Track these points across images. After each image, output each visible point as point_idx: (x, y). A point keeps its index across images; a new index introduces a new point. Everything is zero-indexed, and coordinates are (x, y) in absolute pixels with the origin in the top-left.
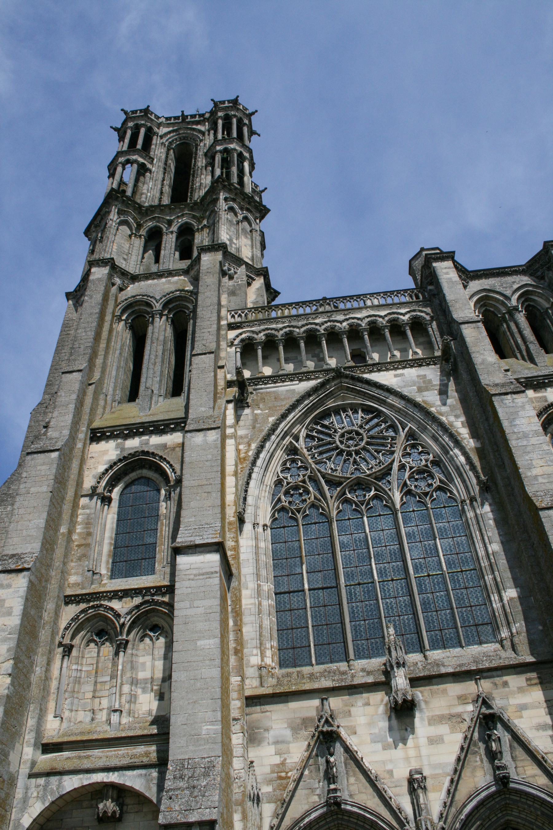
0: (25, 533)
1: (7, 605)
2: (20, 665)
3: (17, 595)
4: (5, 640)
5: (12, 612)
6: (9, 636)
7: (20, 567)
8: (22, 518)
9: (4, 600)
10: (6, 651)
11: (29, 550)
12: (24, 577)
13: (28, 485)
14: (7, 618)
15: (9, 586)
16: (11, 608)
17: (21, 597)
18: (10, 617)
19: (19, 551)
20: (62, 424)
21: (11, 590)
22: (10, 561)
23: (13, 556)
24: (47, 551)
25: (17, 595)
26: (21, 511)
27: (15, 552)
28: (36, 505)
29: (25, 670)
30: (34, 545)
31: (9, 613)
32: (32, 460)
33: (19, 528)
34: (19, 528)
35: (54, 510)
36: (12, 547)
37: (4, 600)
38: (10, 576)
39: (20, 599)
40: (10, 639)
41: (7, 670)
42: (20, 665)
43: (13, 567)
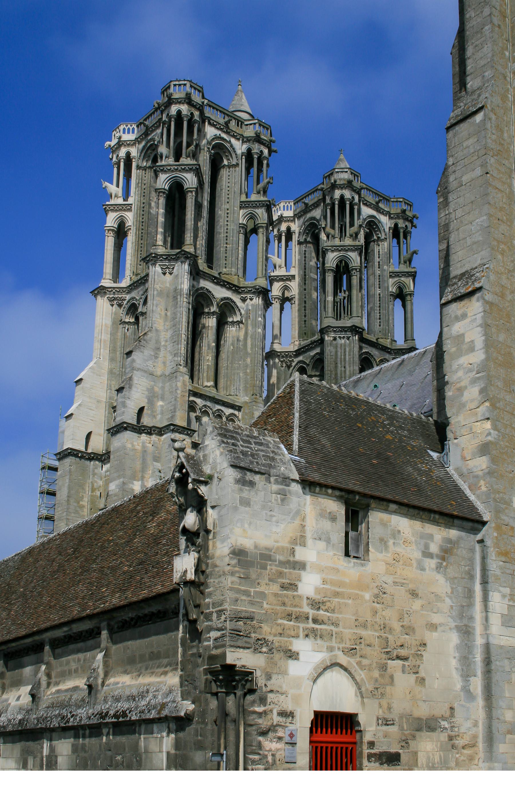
0: (469, 241)
1: (467, 339)
2: (500, 405)
3: (475, 324)
4: (474, 381)
5: (474, 347)
6: (477, 375)
7: (470, 289)
8: (461, 222)
9: (463, 335)
10: (478, 393)
11: (479, 262)
12: (478, 300)
13: (458, 174)
14: (471, 355)
15: (464, 316)
16: (472, 341)
17: (480, 326)
18: (473, 354)
19: (467, 267)
20: (482, 63)
21: (467, 320)
22: (460, 283)
23: (463, 275)
24: (502, 254)
25: (475, 324)
26: (459, 213)
27: (463, 270)
28: (473, 198)
29: (508, 408)
30: (483, 253)
31: (472, 349)
32: (454, 136)
33: (461, 236)
34: (461, 236)
35: (499, 195)
36: (459, 265)
37: (463, 335)
38: (463, 303)
39: (479, 329)
40: (479, 378)
41: (484, 414)
42: (500, 405)
43: (463, 291)
